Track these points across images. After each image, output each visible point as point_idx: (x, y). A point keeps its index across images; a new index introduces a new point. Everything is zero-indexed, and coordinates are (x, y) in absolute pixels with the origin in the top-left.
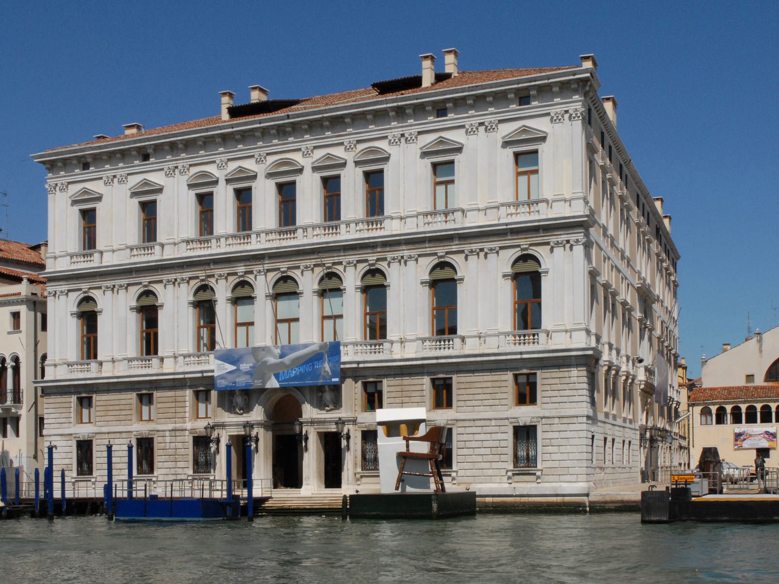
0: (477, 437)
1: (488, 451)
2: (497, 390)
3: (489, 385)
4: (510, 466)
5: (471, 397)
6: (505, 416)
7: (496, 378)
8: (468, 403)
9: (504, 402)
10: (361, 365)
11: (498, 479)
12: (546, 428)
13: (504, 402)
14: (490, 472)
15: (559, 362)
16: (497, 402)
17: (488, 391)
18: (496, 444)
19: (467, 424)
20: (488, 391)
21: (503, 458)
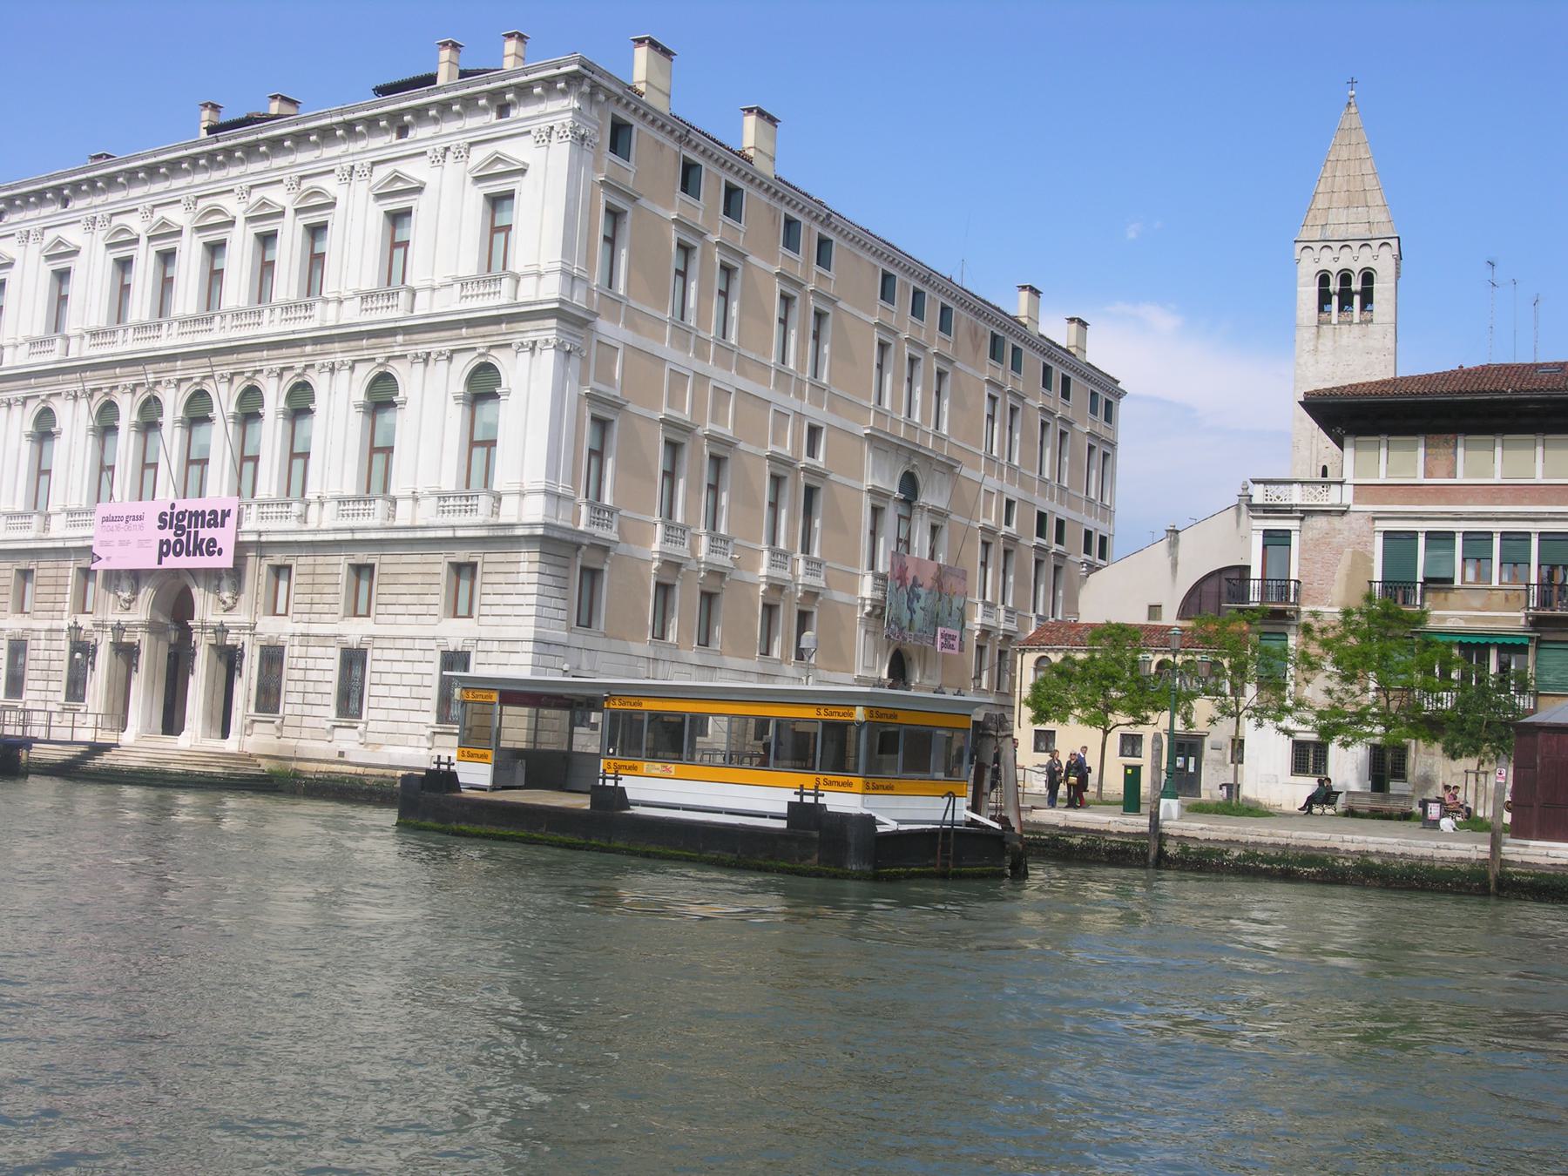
0: (398, 667)
1: (405, 692)
2: (426, 589)
3: (418, 579)
4: (432, 719)
5: (393, 599)
6: (430, 634)
7: (426, 569)
8: (391, 609)
9: (433, 610)
10: (264, 538)
11: (413, 740)
12: (482, 657)
13: (433, 610)
14: (407, 728)
15: (502, 540)
16: (424, 609)
17: (415, 589)
18: (416, 680)
19: (386, 644)
20: (415, 589)
21: (426, 705)
